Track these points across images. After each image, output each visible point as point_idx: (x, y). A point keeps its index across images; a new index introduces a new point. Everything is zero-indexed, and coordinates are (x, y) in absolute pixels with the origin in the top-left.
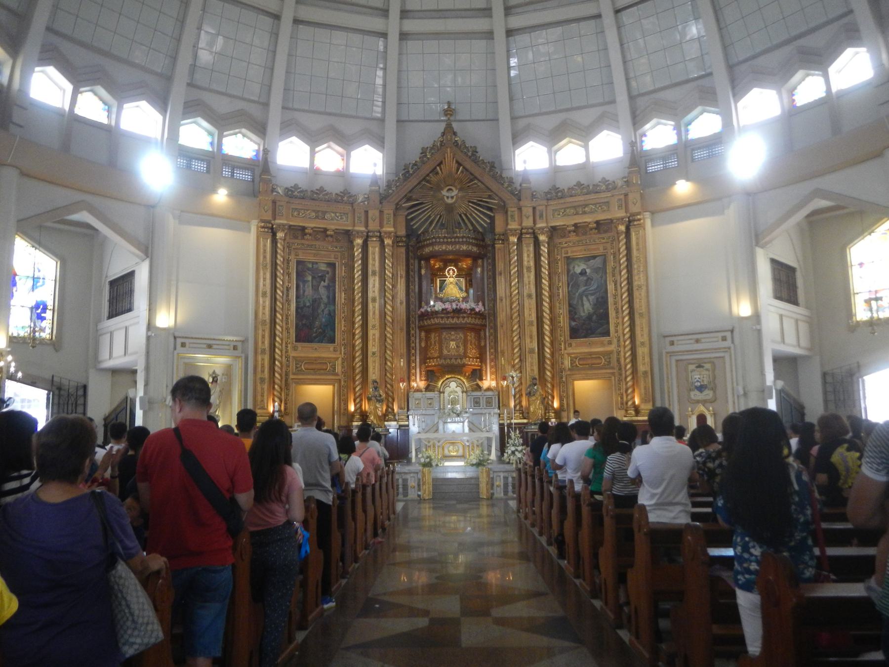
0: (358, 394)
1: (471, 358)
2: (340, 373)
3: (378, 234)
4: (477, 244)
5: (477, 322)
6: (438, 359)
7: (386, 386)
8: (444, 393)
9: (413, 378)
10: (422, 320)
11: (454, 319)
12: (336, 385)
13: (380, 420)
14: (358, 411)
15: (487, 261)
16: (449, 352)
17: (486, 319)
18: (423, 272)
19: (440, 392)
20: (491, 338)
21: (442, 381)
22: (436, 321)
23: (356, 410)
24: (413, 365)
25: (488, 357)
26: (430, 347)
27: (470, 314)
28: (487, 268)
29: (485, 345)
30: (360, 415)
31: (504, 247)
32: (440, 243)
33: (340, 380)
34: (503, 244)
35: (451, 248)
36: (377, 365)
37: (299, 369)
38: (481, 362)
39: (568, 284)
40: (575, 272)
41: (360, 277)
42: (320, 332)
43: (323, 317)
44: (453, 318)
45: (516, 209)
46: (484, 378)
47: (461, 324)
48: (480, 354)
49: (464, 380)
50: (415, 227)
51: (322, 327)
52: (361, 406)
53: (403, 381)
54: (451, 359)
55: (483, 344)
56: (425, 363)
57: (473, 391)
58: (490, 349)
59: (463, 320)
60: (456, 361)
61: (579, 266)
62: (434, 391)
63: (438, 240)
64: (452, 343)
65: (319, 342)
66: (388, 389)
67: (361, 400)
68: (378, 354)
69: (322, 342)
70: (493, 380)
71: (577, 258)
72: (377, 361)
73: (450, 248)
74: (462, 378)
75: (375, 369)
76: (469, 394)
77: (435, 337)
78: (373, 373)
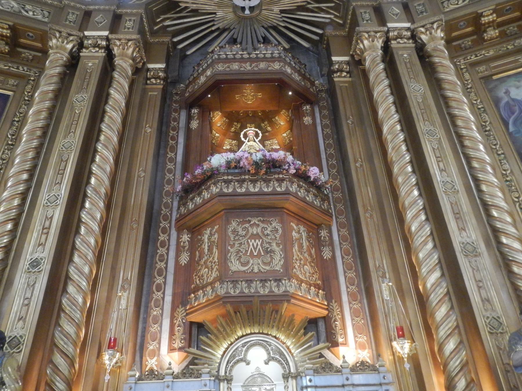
1: (302, 281)
3: (104, 43)
4: (299, 71)
5: (310, 198)
6: (217, 284)
8: (229, 380)
9: (151, 346)
10: (185, 204)
11: (258, 185)
15: (320, 113)
16: (243, 265)
17: (329, 202)
18: (194, 124)
19: (218, 379)
20: (346, 246)
21: (225, 345)
22: (215, 190)
24: (155, 312)
25: (343, 288)
26: (198, 263)
27: (295, 175)
28: (321, 123)
29: (334, 257)
31: (352, 83)
32: (227, 60)
34: (350, 77)
35: (249, 68)
38: (329, 297)
39: (506, 124)
40: (513, 100)
41: (47, 104)
44: (254, 182)
45: (370, 10)
46: (340, 340)
47: (274, 193)
48: (323, 281)
49: (289, 343)
50: (180, 46)
53: (113, 345)
54: (249, 282)
55: (327, 254)
56: (184, 302)
57: (316, 372)
58: (345, 272)
59: (280, 186)
60: (264, 286)
61: (518, 88)
62: (199, 376)
63: (224, 56)
64: (252, 242)
70: (362, 347)
71: (509, 77)
73: (248, 67)
74: (282, 337)
75: (28, 305)
76: (305, 381)
77: (211, 235)
78: (20, 319)
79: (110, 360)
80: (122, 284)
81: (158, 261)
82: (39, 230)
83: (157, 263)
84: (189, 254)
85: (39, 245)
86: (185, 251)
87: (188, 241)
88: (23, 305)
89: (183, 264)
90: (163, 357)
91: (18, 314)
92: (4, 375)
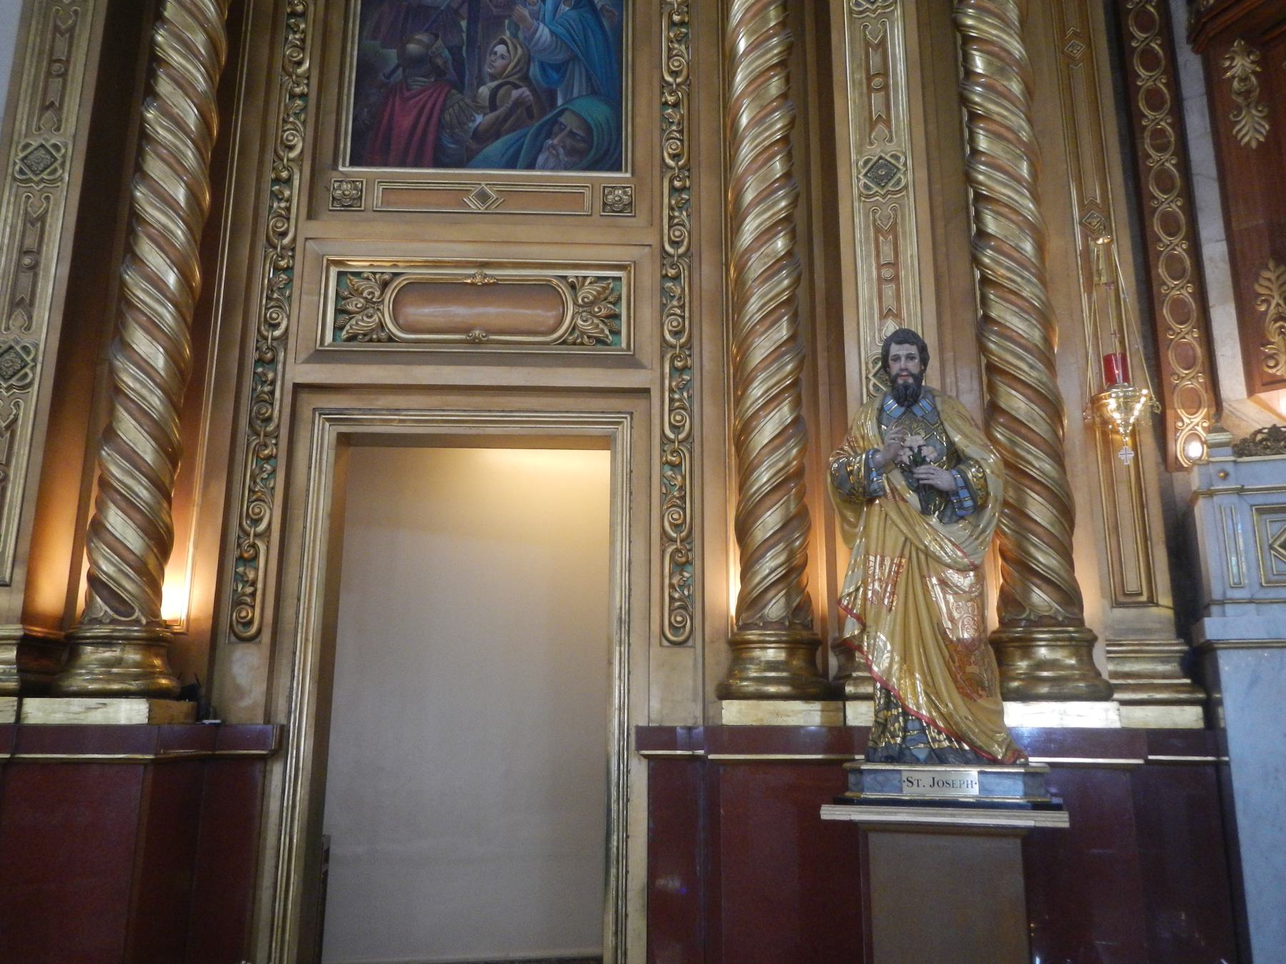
0: (764, 477)
2: (649, 351)
7: (993, 410)
12: (624, 433)
13: (970, 688)
14: (775, 608)
23: (750, 602)
30: (792, 646)
33: (646, 391)
36: (913, 249)
37: (362, 323)
42: (518, 103)
43: (536, 16)
51: (534, 71)
52: (793, 573)
65: (511, 165)
66: (1015, 424)
67: (797, 522)
68: (911, 174)
69: (531, 166)
72: (910, 225)
75: (896, 279)
79: (1126, 407)
80: (1081, 218)
81: (1151, 152)
82: (861, 84)
83: (1149, 156)
84: (1266, 110)
85: (872, 124)
86: (1252, 105)
87: (1254, 73)
88: (881, 280)
89: (1254, 144)
90: (1234, 405)
91: (876, 303)
92: (957, 438)
